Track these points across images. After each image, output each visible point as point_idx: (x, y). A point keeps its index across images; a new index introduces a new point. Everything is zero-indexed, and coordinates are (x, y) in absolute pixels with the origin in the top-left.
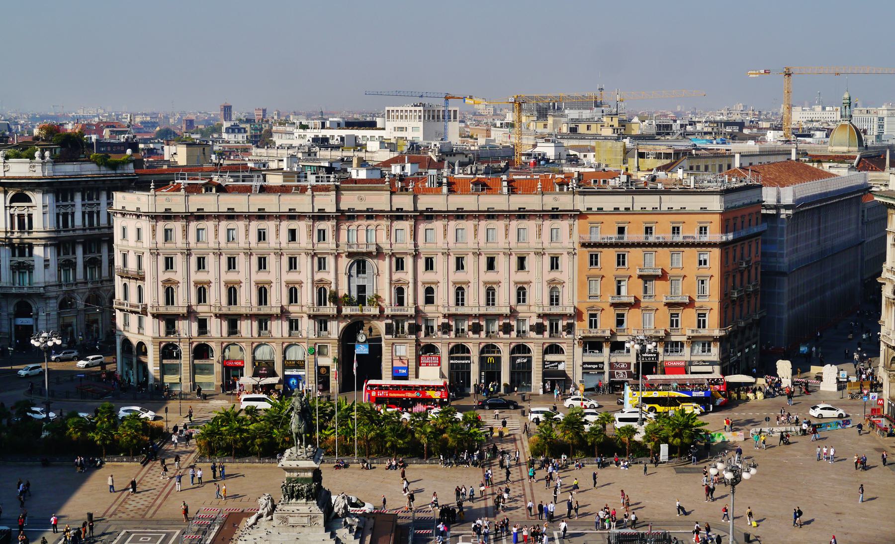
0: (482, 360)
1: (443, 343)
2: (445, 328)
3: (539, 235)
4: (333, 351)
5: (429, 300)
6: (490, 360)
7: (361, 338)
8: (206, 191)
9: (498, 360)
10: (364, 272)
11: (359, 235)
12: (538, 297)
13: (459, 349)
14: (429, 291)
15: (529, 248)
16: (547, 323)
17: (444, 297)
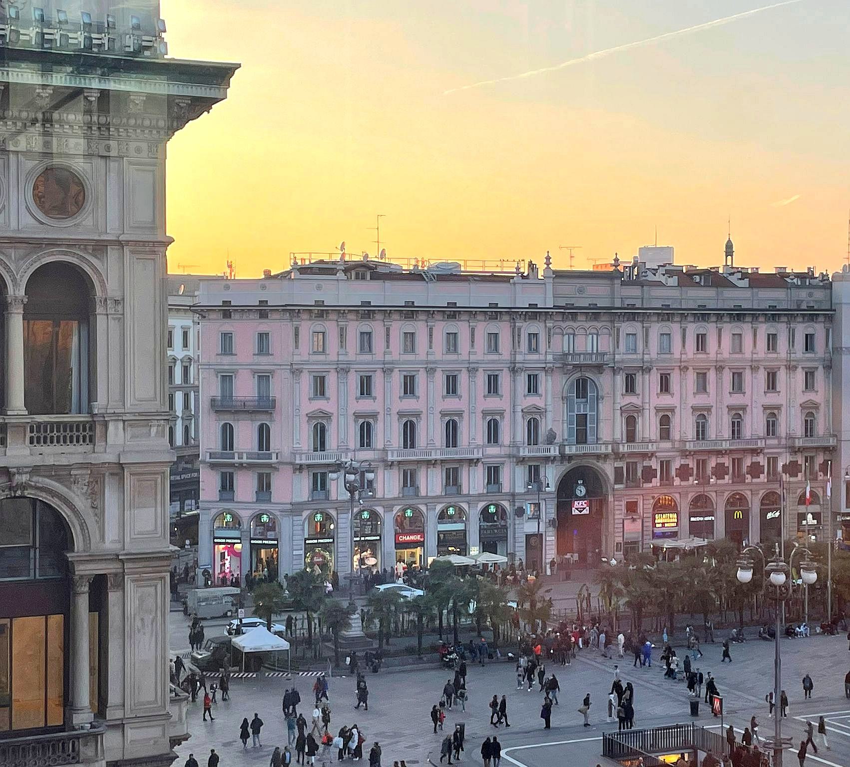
0: (729, 515)
1: (684, 491)
2: (684, 473)
3: (792, 341)
4: (549, 511)
5: (665, 434)
6: (738, 514)
7: (581, 491)
8: (357, 278)
9: (746, 513)
10: (585, 396)
11: (588, 341)
12: (791, 423)
13: (701, 504)
14: (665, 421)
15: (781, 360)
16: (800, 460)
17: (684, 427)
